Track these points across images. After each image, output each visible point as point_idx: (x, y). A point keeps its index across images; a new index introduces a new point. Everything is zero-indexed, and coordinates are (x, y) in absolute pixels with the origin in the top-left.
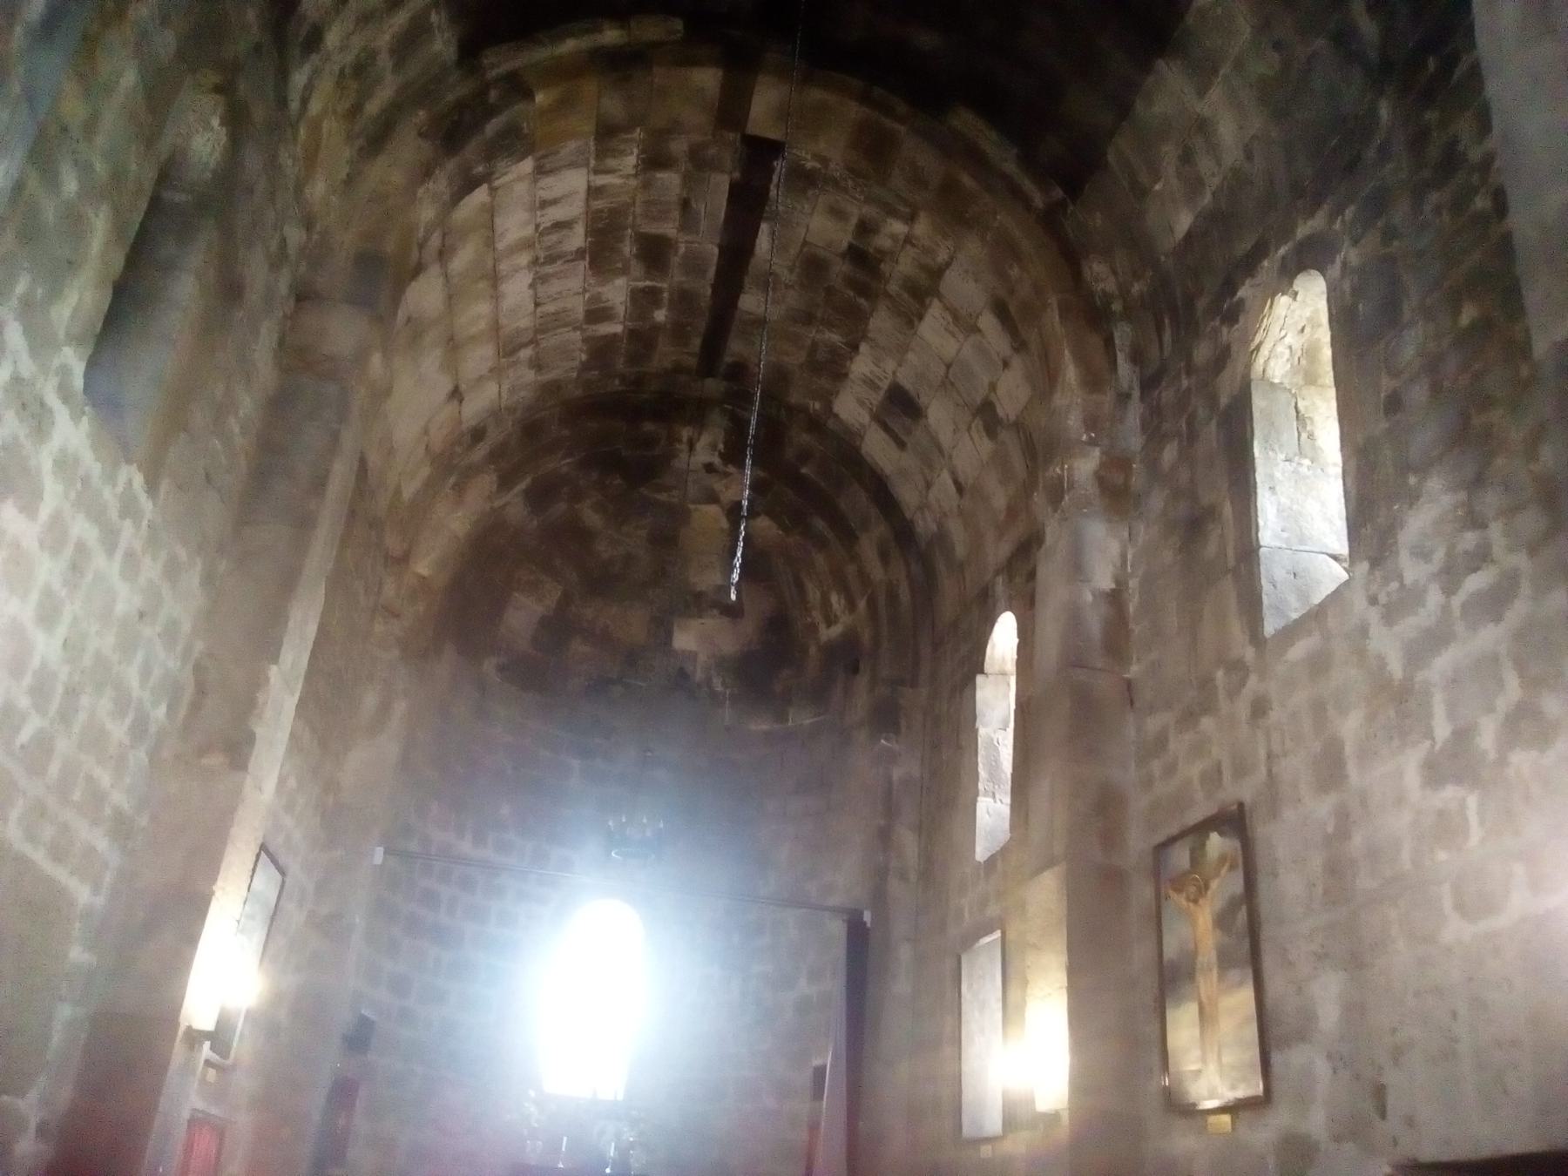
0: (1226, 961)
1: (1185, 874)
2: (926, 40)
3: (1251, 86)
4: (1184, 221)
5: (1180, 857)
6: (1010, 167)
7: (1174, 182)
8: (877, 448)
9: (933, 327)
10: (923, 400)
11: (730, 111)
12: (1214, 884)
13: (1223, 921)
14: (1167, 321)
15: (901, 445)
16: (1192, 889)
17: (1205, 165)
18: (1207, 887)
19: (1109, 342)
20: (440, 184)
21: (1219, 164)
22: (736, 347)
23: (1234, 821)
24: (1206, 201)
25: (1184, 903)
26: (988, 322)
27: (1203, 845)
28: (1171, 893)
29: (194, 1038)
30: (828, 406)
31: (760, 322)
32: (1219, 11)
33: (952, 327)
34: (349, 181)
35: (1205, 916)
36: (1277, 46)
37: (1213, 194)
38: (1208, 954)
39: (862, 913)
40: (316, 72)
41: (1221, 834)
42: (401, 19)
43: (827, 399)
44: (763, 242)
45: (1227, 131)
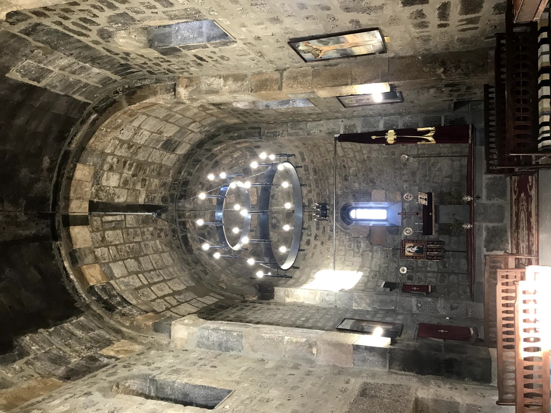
0: (338, 42)
1: (313, 54)
2: (46, 161)
3: (47, 57)
4: (95, 70)
5: (307, 56)
6: (85, 127)
7: (82, 75)
8: (182, 150)
9: (140, 140)
10: (165, 139)
11: (84, 221)
12: (314, 47)
13: (326, 44)
14: (130, 71)
15: (180, 143)
16: (317, 52)
17: (76, 67)
18: (315, 49)
19: (139, 87)
20: (127, 309)
21: (75, 63)
22: (157, 202)
23: (293, 43)
24: (88, 65)
25: (322, 54)
26: (136, 124)
27: (303, 51)
28: (320, 57)
29: (393, 342)
30: (170, 169)
31: (147, 196)
32: (22, 70)
33: (139, 134)
34: (132, 339)
35: (324, 48)
36: (32, 52)
37: (85, 63)
38: (338, 46)
39: (336, 139)
40: (102, 355)
41: (299, 46)
42: (79, 333)
43: (168, 170)
44: (122, 200)
45: (64, 62)
